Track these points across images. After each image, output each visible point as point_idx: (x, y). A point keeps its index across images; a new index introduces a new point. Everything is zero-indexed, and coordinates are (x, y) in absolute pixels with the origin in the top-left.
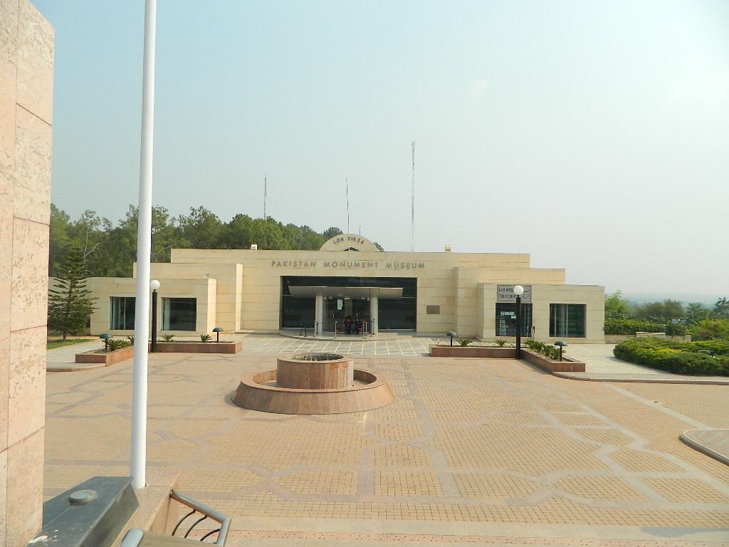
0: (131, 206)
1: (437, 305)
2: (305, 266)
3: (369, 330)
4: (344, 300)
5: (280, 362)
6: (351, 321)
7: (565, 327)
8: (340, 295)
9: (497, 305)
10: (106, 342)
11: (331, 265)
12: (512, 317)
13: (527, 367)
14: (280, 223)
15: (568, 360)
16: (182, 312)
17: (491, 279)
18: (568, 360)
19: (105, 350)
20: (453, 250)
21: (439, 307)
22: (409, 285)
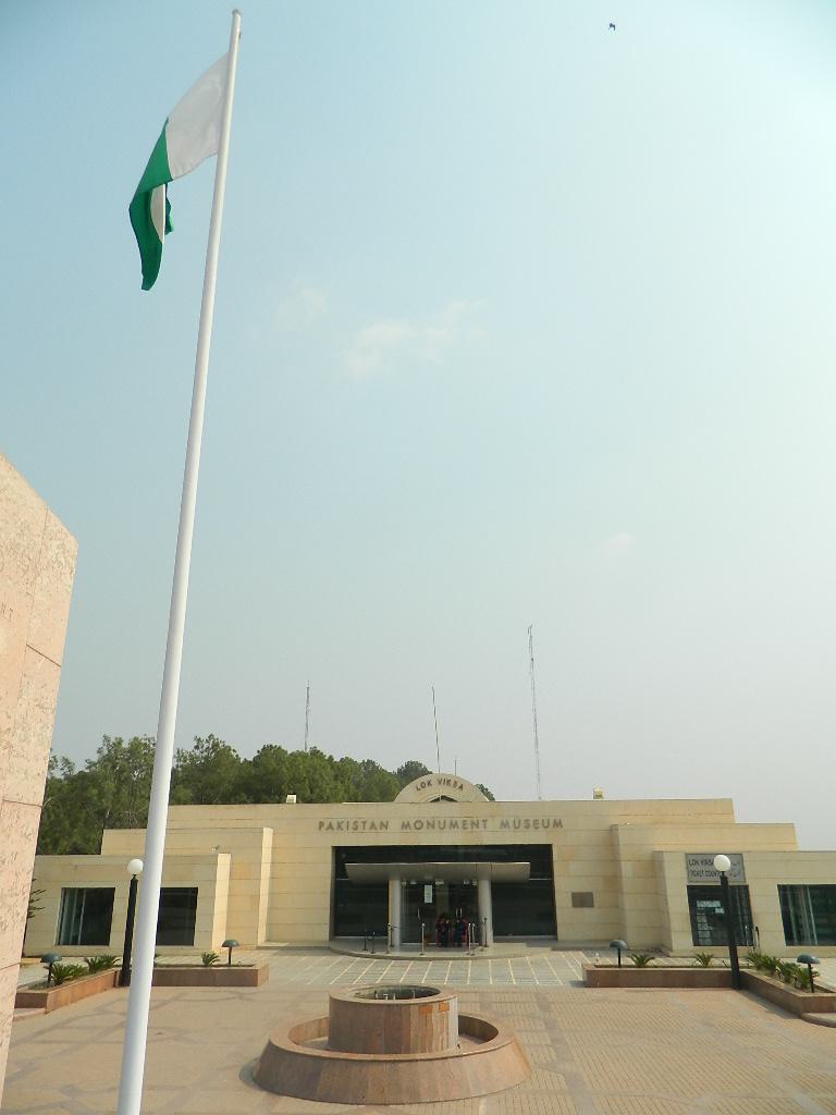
0: (106, 739)
1: (589, 891)
2: (371, 828)
3: (478, 939)
4: (434, 886)
5: (337, 1005)
6: (446, 923)
7: (811, 926)
8: (428, 877)
9: (690, 888)
10: (50, 968)
11: (412, 825)
12: (717, 911)
13: (754, 1003)
14: (331, 758)
15: (827, 991)
17: (675, 844)
18: (827, 991)
19: (46, 985)
20: (606, 797)
21: (590, 895)
22: (540, 856)
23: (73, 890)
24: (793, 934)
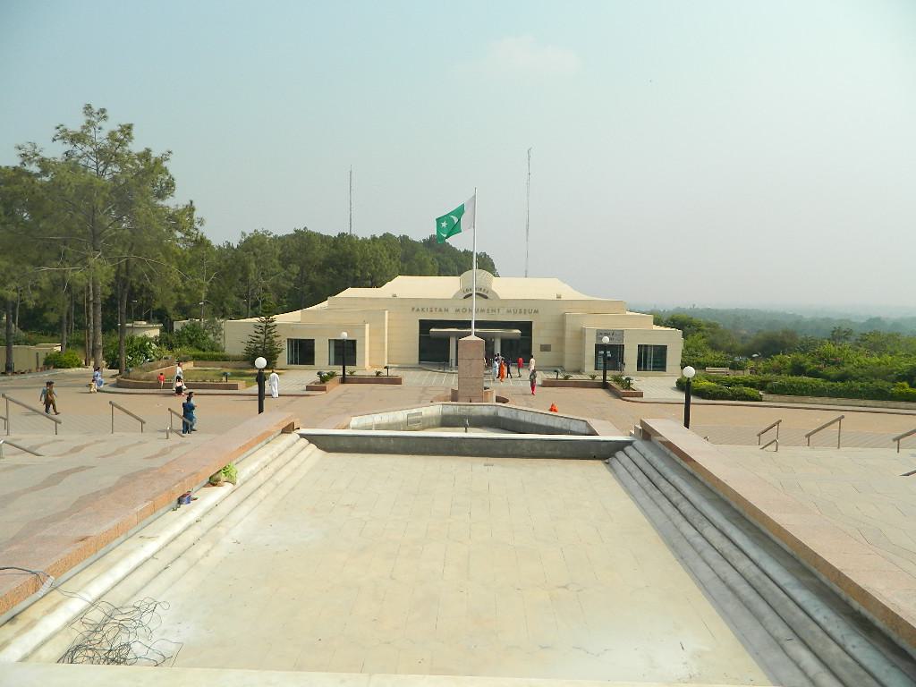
16: (345, 351)
17: (592, 325)
22: (526, 327)
23: (292, 340)
24: (642, 365)
